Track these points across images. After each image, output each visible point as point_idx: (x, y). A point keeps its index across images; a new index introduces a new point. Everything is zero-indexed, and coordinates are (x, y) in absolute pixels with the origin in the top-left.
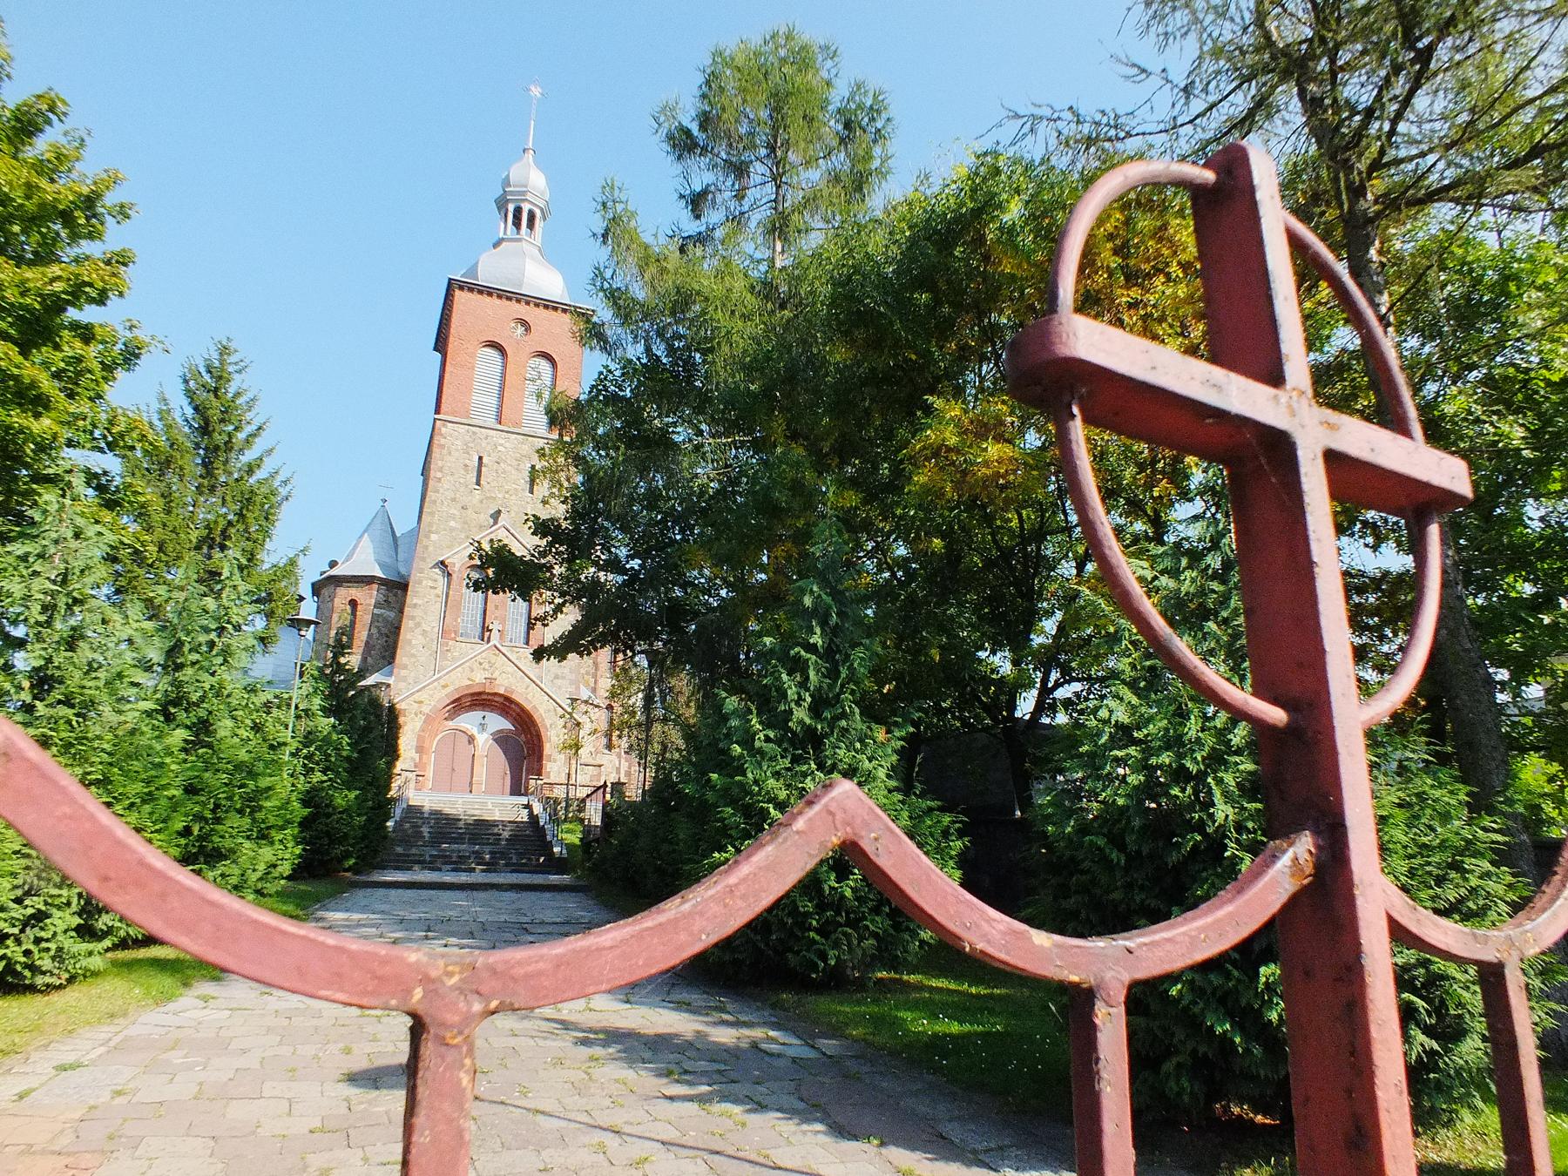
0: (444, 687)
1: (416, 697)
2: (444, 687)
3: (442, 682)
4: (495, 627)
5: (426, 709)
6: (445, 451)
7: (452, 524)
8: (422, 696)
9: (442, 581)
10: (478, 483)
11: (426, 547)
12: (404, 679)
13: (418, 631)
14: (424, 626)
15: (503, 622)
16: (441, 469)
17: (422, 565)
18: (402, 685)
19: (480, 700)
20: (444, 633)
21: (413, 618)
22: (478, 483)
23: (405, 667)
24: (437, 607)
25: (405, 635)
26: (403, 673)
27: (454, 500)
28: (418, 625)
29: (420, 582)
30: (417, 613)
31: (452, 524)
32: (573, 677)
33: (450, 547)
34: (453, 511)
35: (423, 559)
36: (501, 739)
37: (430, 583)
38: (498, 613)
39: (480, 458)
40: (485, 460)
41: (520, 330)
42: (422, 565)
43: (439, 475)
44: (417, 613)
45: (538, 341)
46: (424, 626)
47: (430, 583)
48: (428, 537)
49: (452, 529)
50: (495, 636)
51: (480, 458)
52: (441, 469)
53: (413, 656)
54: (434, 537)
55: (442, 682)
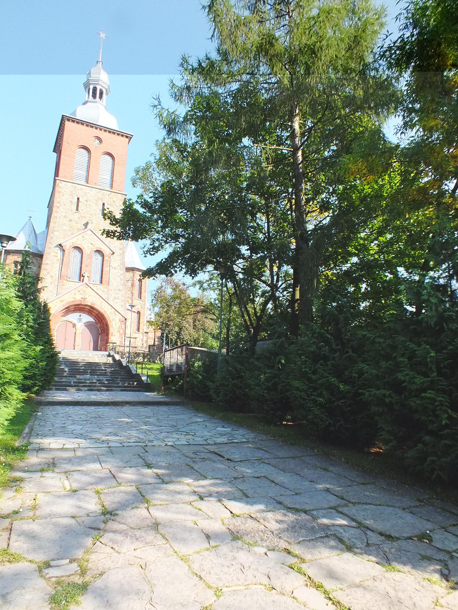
4: (86, 275)
6: (61, 194)
7: (65, 227)
9: (59, 253)
10: (77, 209)
11: (52, 238)
15: (90, 272)
20: (61, 277)
21: (46, 270)
22: (77, 209)
24: (57, 265)
27: (65, 217)
28: (49, 273)
29: (49, 253)
30: (48, 267)
31: (65, 227)
35: (51, 243)
37: (54, 254)
38: (87, 269)
43: (58, 205)
44: (48, 267)
47: (54, 254)
50: (86, 279)
52: (59, 203)
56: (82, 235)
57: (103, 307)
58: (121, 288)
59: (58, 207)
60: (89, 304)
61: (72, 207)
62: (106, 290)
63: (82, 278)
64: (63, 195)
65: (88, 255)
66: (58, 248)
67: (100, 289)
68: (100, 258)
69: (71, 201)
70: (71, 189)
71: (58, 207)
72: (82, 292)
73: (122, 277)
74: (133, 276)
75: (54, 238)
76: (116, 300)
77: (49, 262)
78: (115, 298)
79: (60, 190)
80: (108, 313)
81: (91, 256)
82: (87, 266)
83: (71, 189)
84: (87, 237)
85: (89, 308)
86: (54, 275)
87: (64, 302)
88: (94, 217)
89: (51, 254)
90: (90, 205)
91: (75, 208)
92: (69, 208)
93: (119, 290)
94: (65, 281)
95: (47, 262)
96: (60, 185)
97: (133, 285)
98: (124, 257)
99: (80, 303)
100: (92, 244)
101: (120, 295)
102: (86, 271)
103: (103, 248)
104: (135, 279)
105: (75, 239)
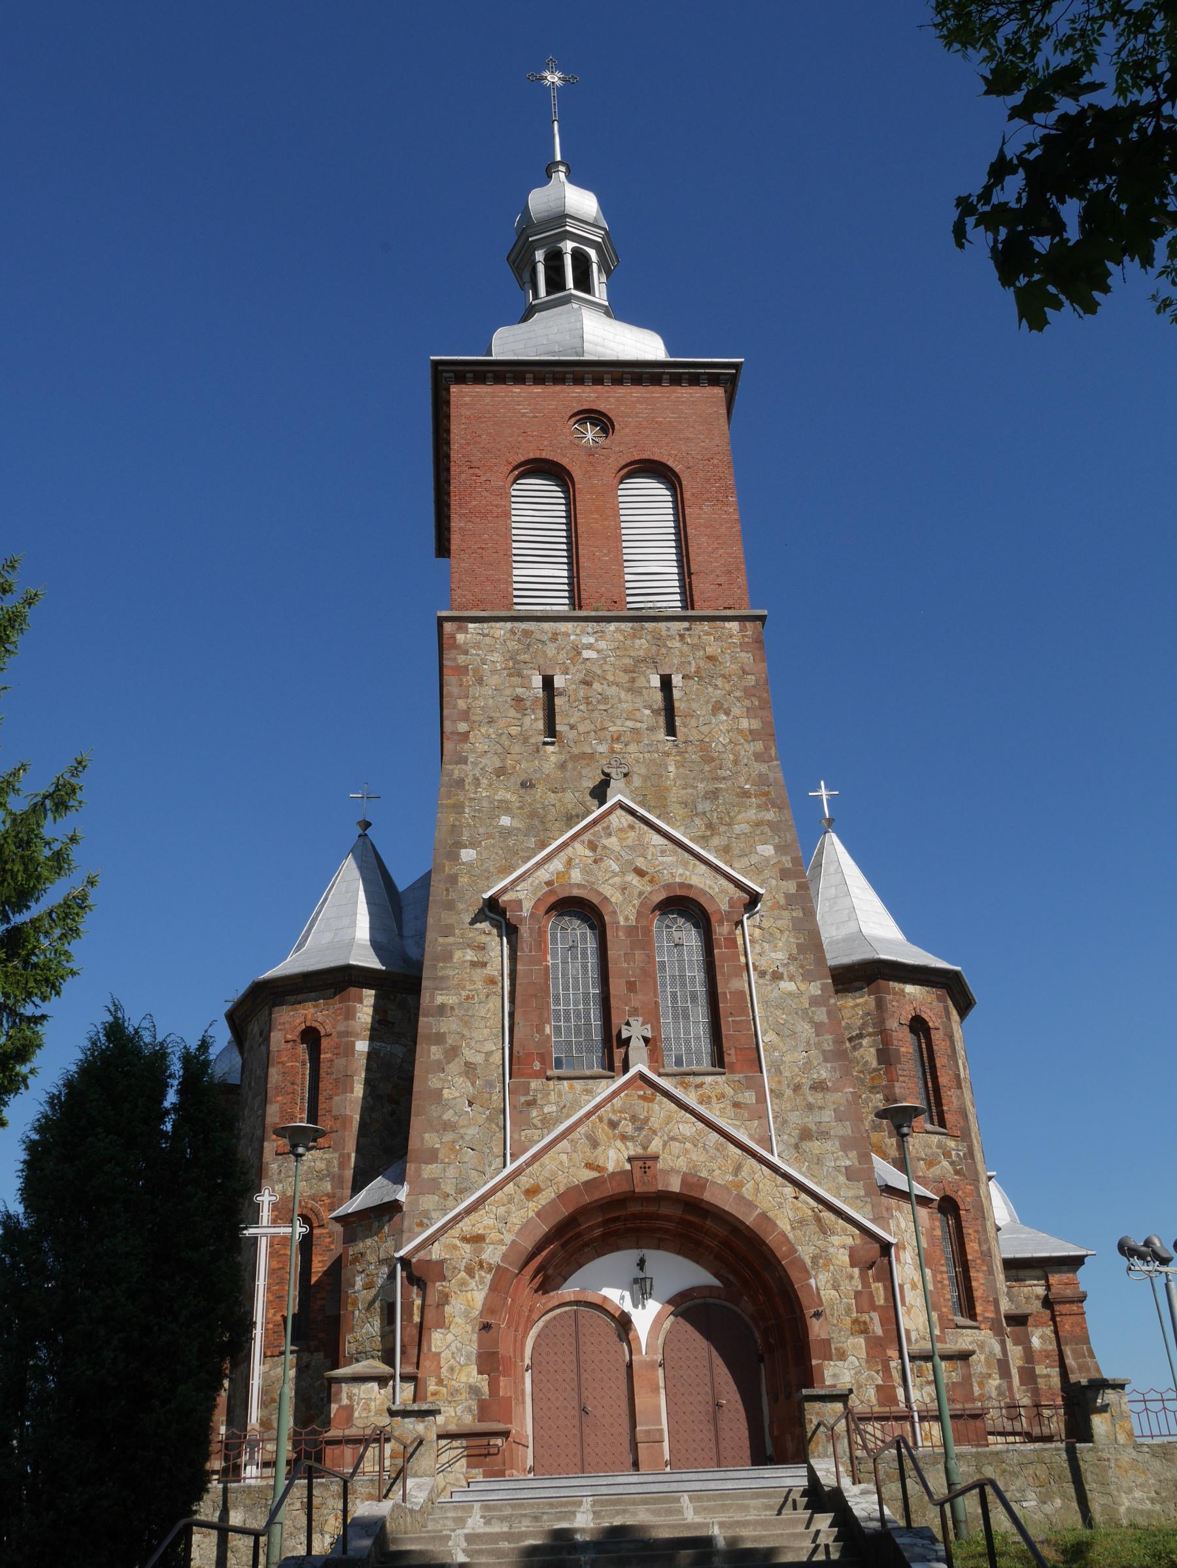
0: (532, 1192)
1: (465, 1226)
2: (532, 1192)
3: (525, 1181)
4: (636, 1030)
5: (492, 1254)
6: (469, 679)
7: (505, 821)
8: (482, 1222)
9: (497, 949)
10: (551, 730)
11: (453, 879)
12: (434, 1186)
13: (454, 1067)
14: (469, 1055)
15: (652, 1016)
16: (465, 716)
17: (448, 918)
18: (429, 1202)
19: (616, 1219)
20: (518, 1063)
21: (439, 1039)
22: (551, 730)
23: (432, 1156)
24: (491, 1010)
25: (426, 1080)
26: (429, 1171)
27: (501, 772)
28: (453, 1053)
29: (447, 956)
30: (449, 1025)
31: (505, 821)
32: (845, 1129)
33: (506, 870)
34: (501, 795)
35: (450, 906)
36: (687, 1307)
37: (470, 955)
38: (636, 1000)
39: (548, 682)
40: (559, 682)
41: (590, 433)
42: (448, 918)
43: (463, 727)
44: (449, 1025)
45: (629, 443)
46: (469, 1055)
47: (470, 955)
48: (454, 857)
49: (506, 833)
51: (548, 682)
52: (465, 716)
53: (448, 1126)
54: (467, 855)
55: (525, 1181)
56: (586, 837)
57: (747, 1191)
58: (823, 1073)
59: (465, 737)
60: (675, 1186)
61: (527, 721)
62: (749, 1097)
63: (618, 1053)
64: (480, 681)
65: (631, 931)
66: (485, 926)
67: (715, 1095)
68: (691, 938)
69: (518, 700)
70: (513, 645)
71: (465, 737)
72: (627, 1127)
73: (821, 1015)
74: (880, 1005)
75: (463, 880)
76: (815, 1146)
77: (451, 1000)
78: (806, 1135)
79: (462, 659)
80: (784, 1225)
81: (647, 931)
82: (631, 987)
83: (513, 645)
84: (612, 842)
85: (674, 1211)
86: (479, 1059)
87: (547, 1196)
88: (632, 748)
89: (457, 955)
90: (605, 699)
91: (540, 725)
92: (514, 730)
93: (819, 1086)
94: (534, 1084)
95: (440, 999)
96: (460, 638)
97: (886, 1056)
98: (810, 913)
99: (626, 1188)
100: (640, 873)
101: (827, 1116)
102: (635, 1012)
103: (695, 881)
104: (892, 1024)
105: (557, 865)
